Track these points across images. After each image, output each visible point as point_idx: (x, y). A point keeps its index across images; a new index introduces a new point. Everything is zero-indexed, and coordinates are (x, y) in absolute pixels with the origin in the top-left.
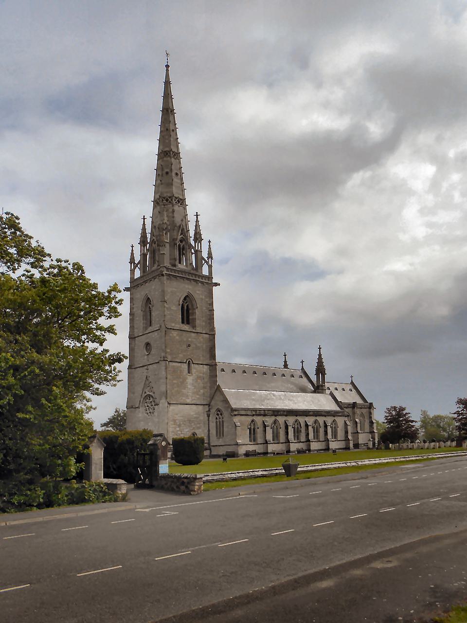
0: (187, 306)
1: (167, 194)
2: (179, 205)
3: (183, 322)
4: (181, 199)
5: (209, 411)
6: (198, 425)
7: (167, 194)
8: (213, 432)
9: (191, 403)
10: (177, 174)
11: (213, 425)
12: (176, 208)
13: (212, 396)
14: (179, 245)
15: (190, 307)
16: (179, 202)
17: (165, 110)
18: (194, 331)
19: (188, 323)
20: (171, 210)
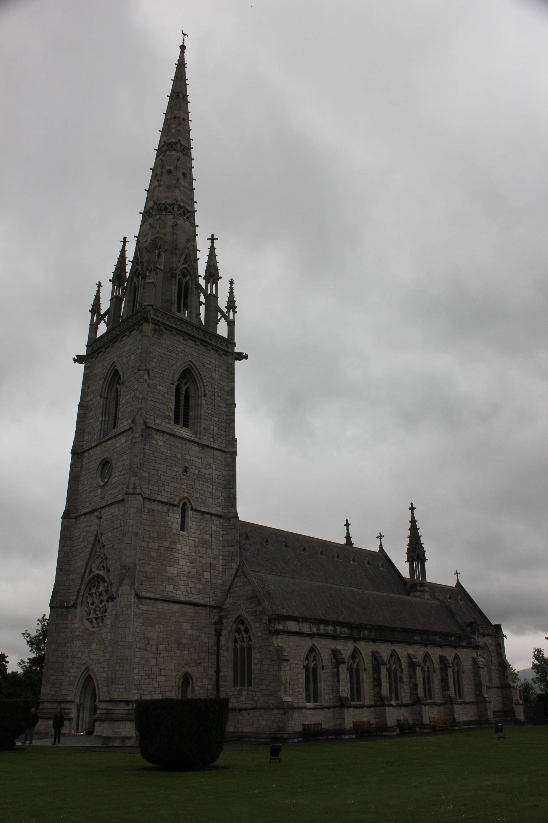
0: (187, 391)
1: (166, 200)
2: (185, 217)
3: (177, 422)
4: (189, 212)
5: (220, 622)
6: (195, 656)
7: (166, 200)
8: (227, 673)
9: (182, 598)
10: (184, 175)
11: (227, 656)
12: (180, 221)
13: (227, 587)
14: (180, 279)
15: (192, 394)
16: (184, 214)
17: (174, 95)
18: (197, 440)
19: (186, 425)
20: (170, 224)
